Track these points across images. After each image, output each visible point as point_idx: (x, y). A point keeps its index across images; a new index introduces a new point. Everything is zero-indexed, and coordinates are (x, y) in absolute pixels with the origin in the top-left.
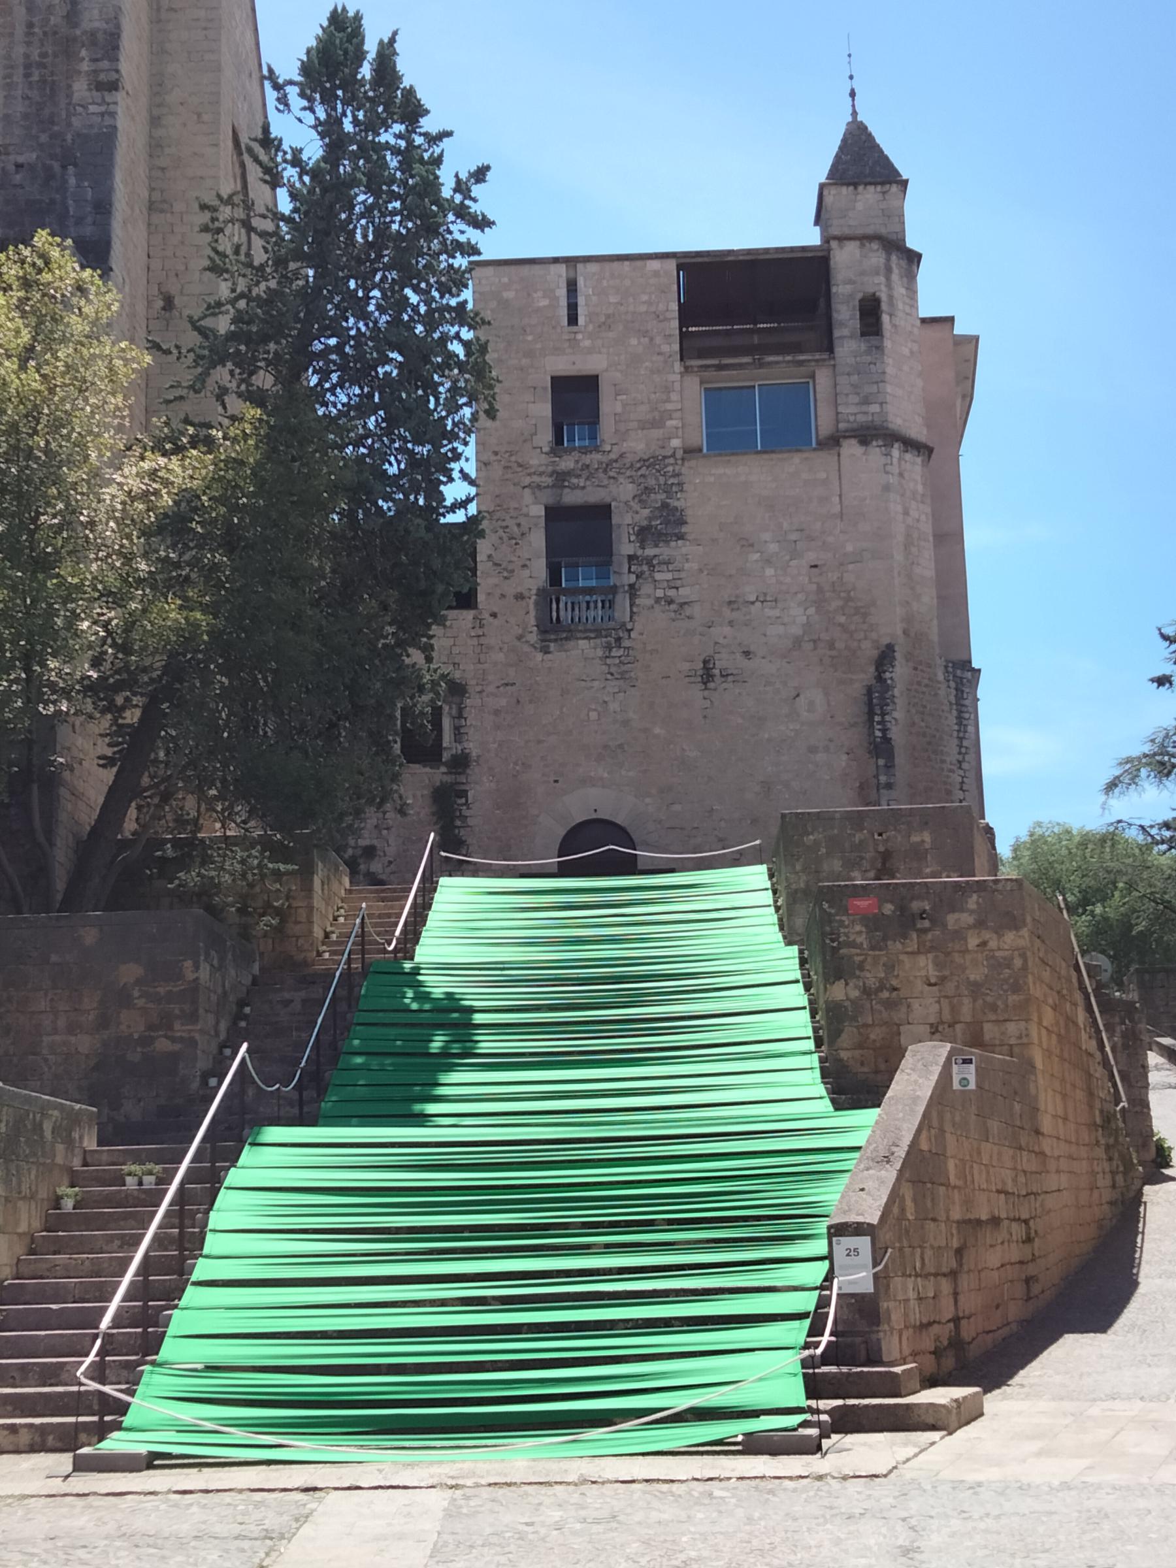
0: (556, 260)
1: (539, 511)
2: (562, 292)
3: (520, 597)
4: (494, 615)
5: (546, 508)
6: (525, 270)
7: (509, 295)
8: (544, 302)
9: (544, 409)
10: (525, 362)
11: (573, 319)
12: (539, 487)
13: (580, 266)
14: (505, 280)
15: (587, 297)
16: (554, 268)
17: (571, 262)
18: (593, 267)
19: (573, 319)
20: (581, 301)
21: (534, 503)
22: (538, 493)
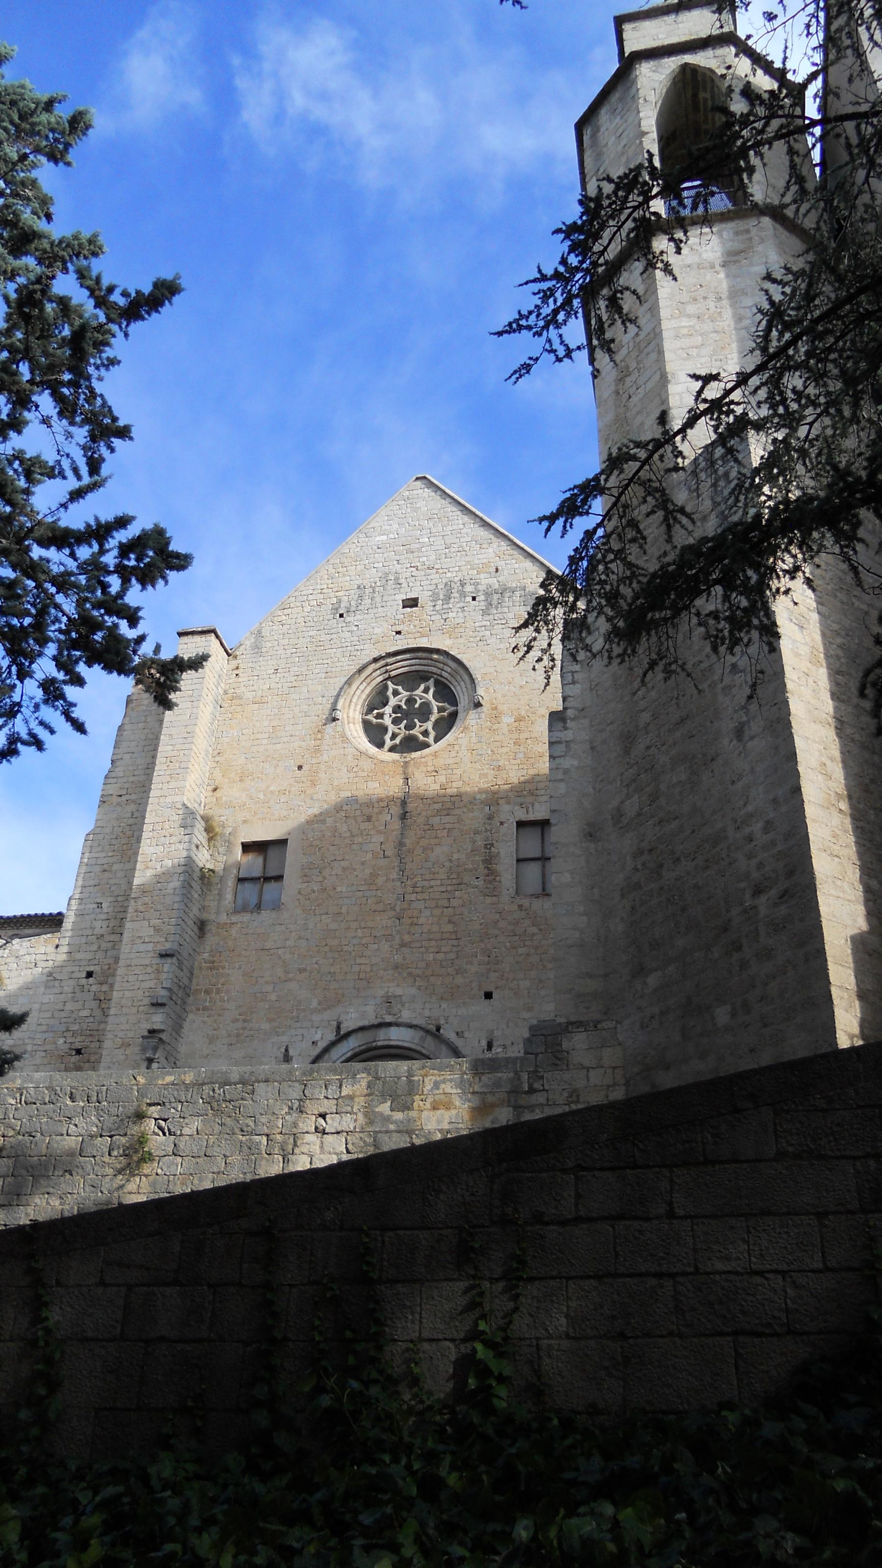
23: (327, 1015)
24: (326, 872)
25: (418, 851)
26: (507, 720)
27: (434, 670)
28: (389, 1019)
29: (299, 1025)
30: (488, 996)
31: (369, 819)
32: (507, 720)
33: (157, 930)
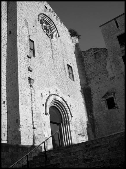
0: (112, 20)
1: (121, 58)
2: (115, 24)
3: (122, 73)
4: (118, 78)
5: (122, 57)
6: (108, 24)
7: (106, 28)
8: (113, 26)
9: (117, 42)
10: (112, 36)
11: (118, 27)
12: (120, 54)
13: (117, 19)
14: (106, 26)
15: (119, 22)
16: (112, 21)
17: (115, 19)
18: (118, 18)
19: (118, 27)
20: (118, 23)
21: (120, 57)
22: (120, 55)
23: (47, 89)
24: (42, 54)
25: (55, 60)
26: (62, 43)
27: (50, 24)
28: (57, 94)
29: (43, 89)
30: (69, 96)
31: (47, 47)
32: (62, 43)
33: (25, 49)
